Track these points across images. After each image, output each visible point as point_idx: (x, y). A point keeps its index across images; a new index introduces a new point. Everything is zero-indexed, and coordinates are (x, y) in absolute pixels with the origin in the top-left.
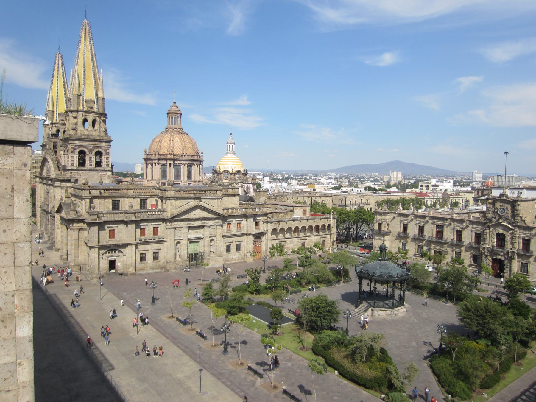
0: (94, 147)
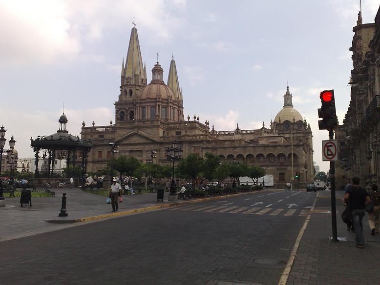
0: (129, 108)
